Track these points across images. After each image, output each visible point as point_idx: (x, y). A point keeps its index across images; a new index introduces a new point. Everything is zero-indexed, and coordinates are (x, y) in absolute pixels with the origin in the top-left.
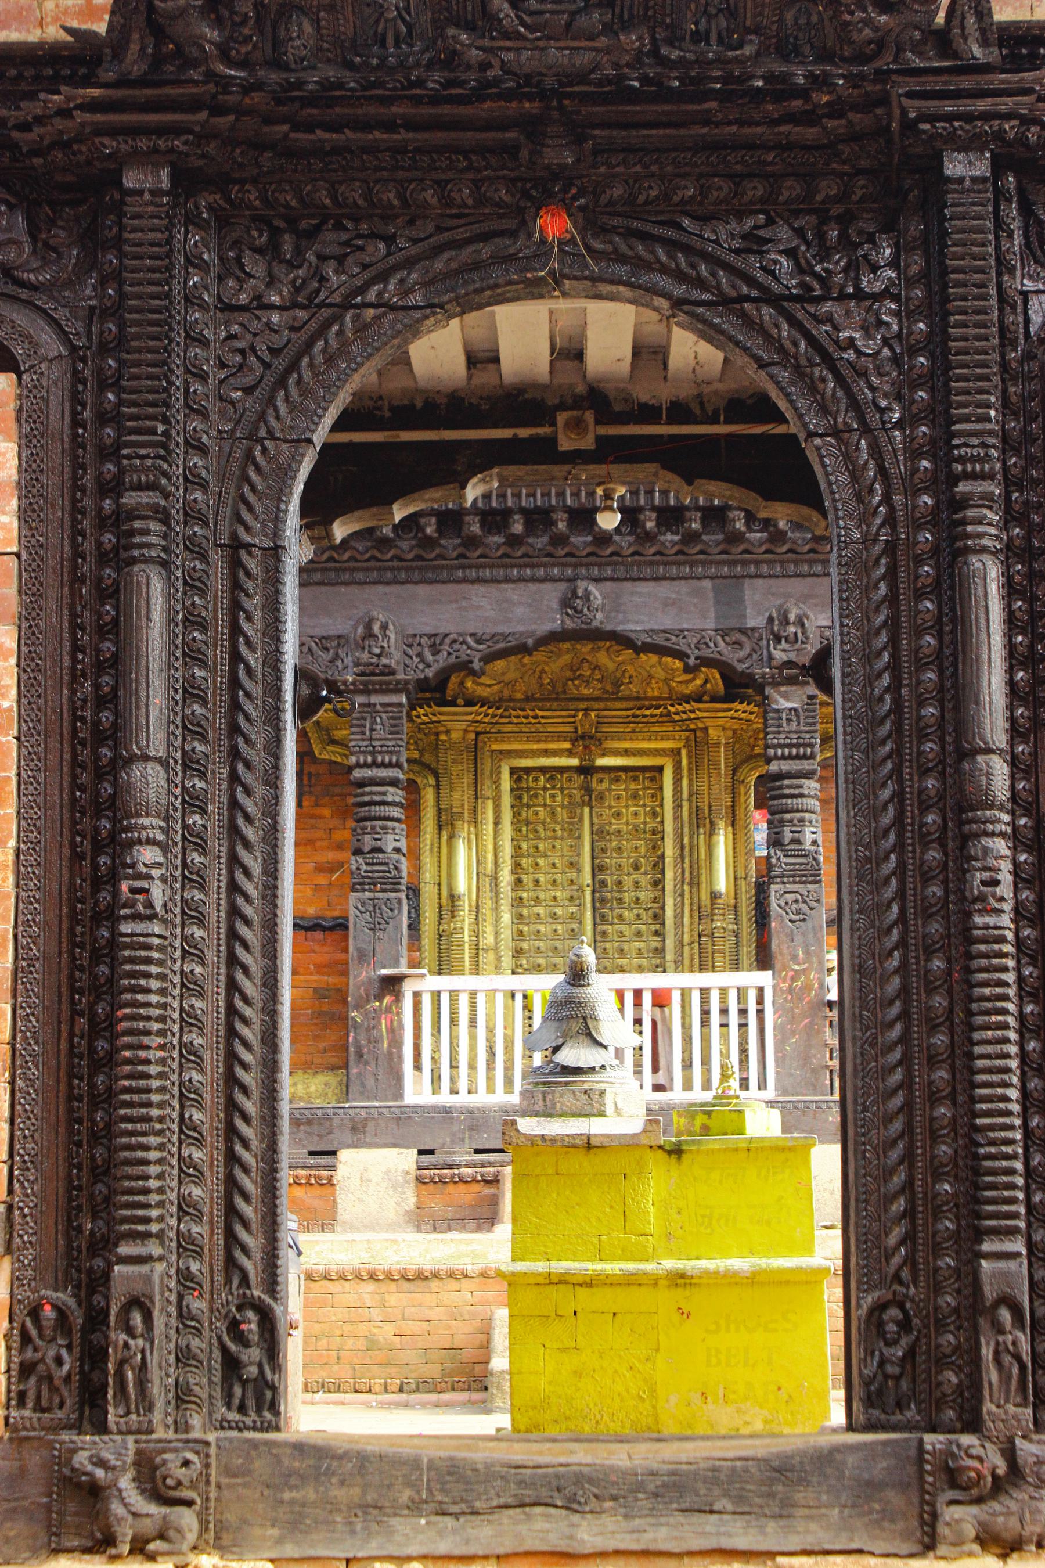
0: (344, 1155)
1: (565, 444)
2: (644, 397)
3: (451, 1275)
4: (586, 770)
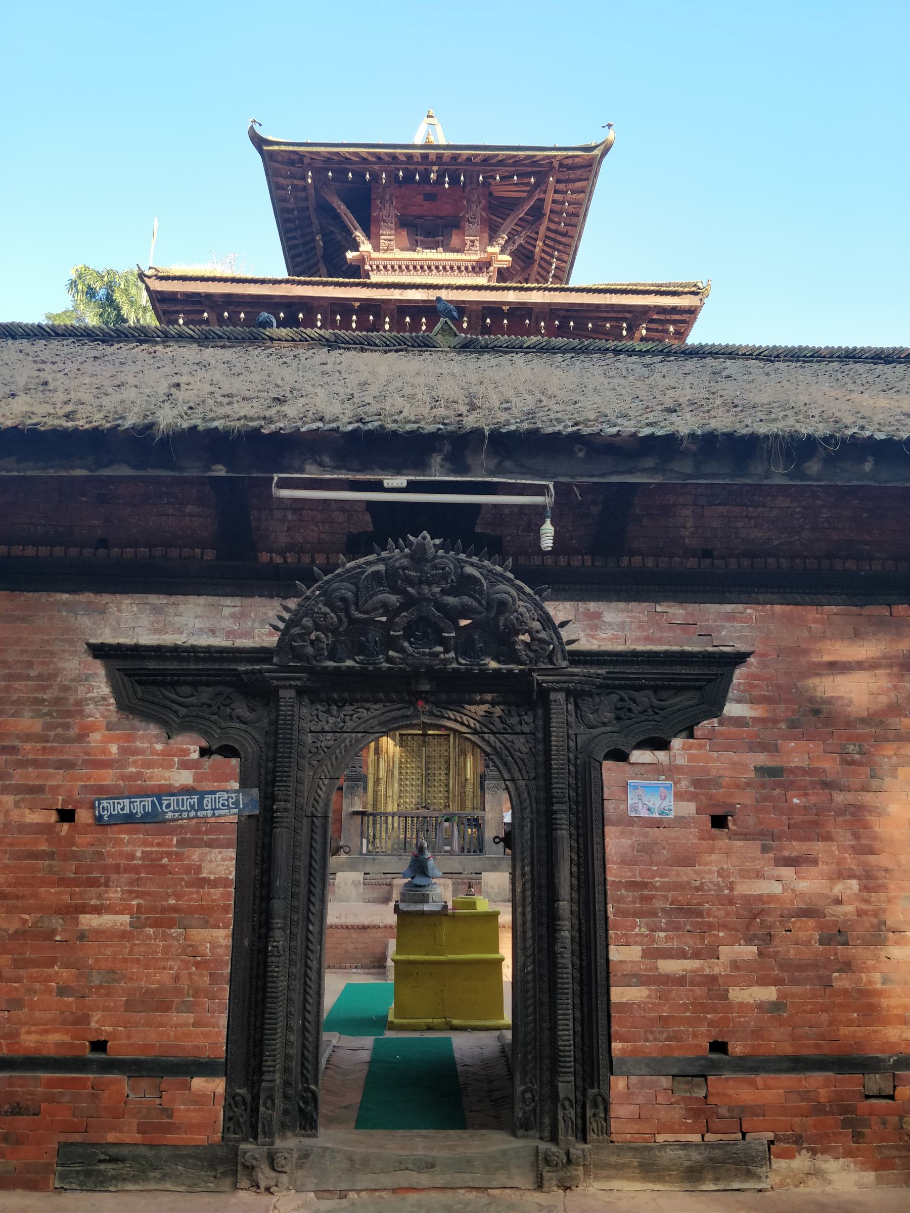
0: (338, 874)
3: (374, 927)
4: (425, 735)
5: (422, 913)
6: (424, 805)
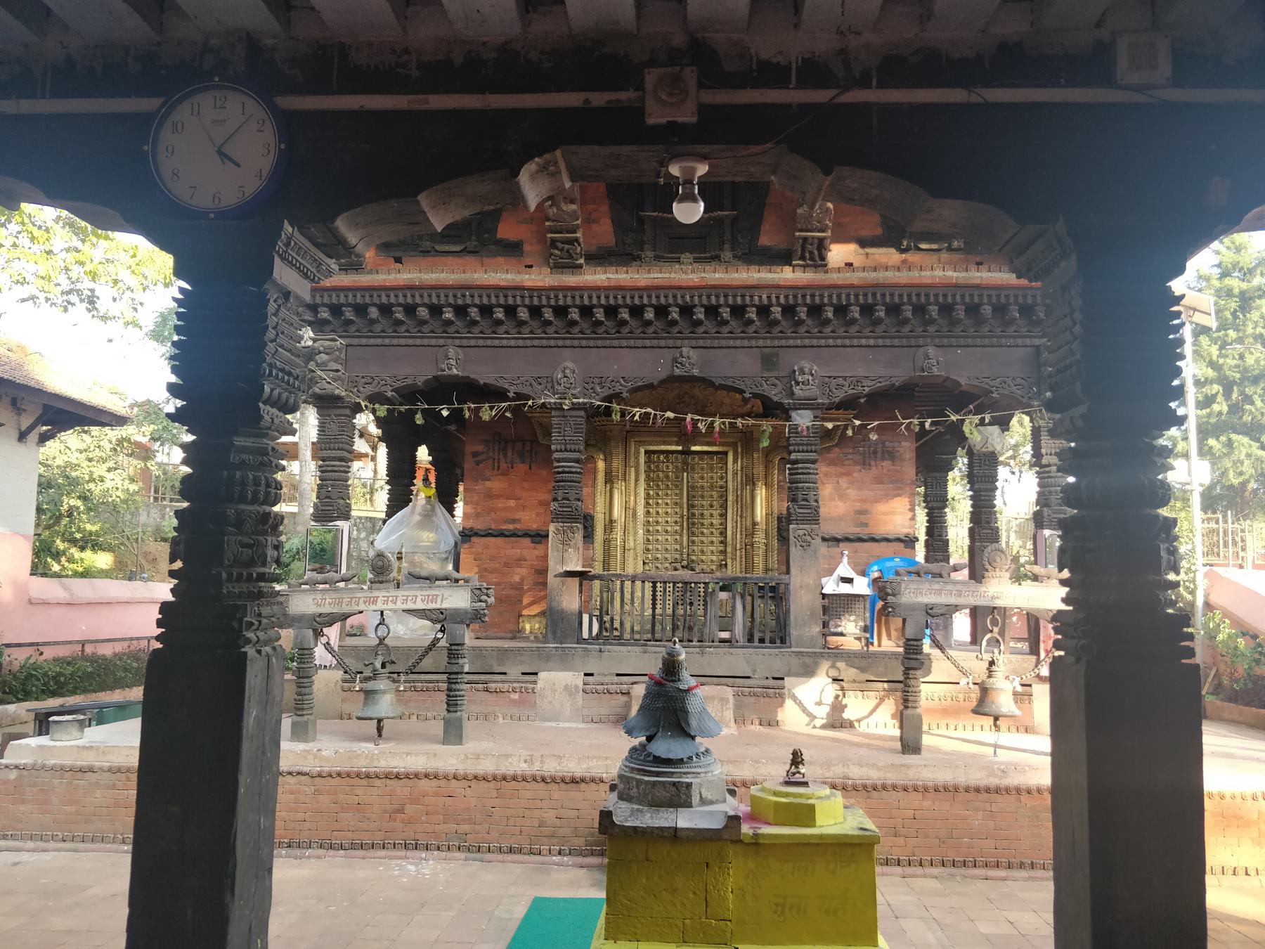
0: (542, 675)
1: (656, 116)
2: (766, 53)
3: (593, 780)
5: (674, 835)
6: (685, 563)
